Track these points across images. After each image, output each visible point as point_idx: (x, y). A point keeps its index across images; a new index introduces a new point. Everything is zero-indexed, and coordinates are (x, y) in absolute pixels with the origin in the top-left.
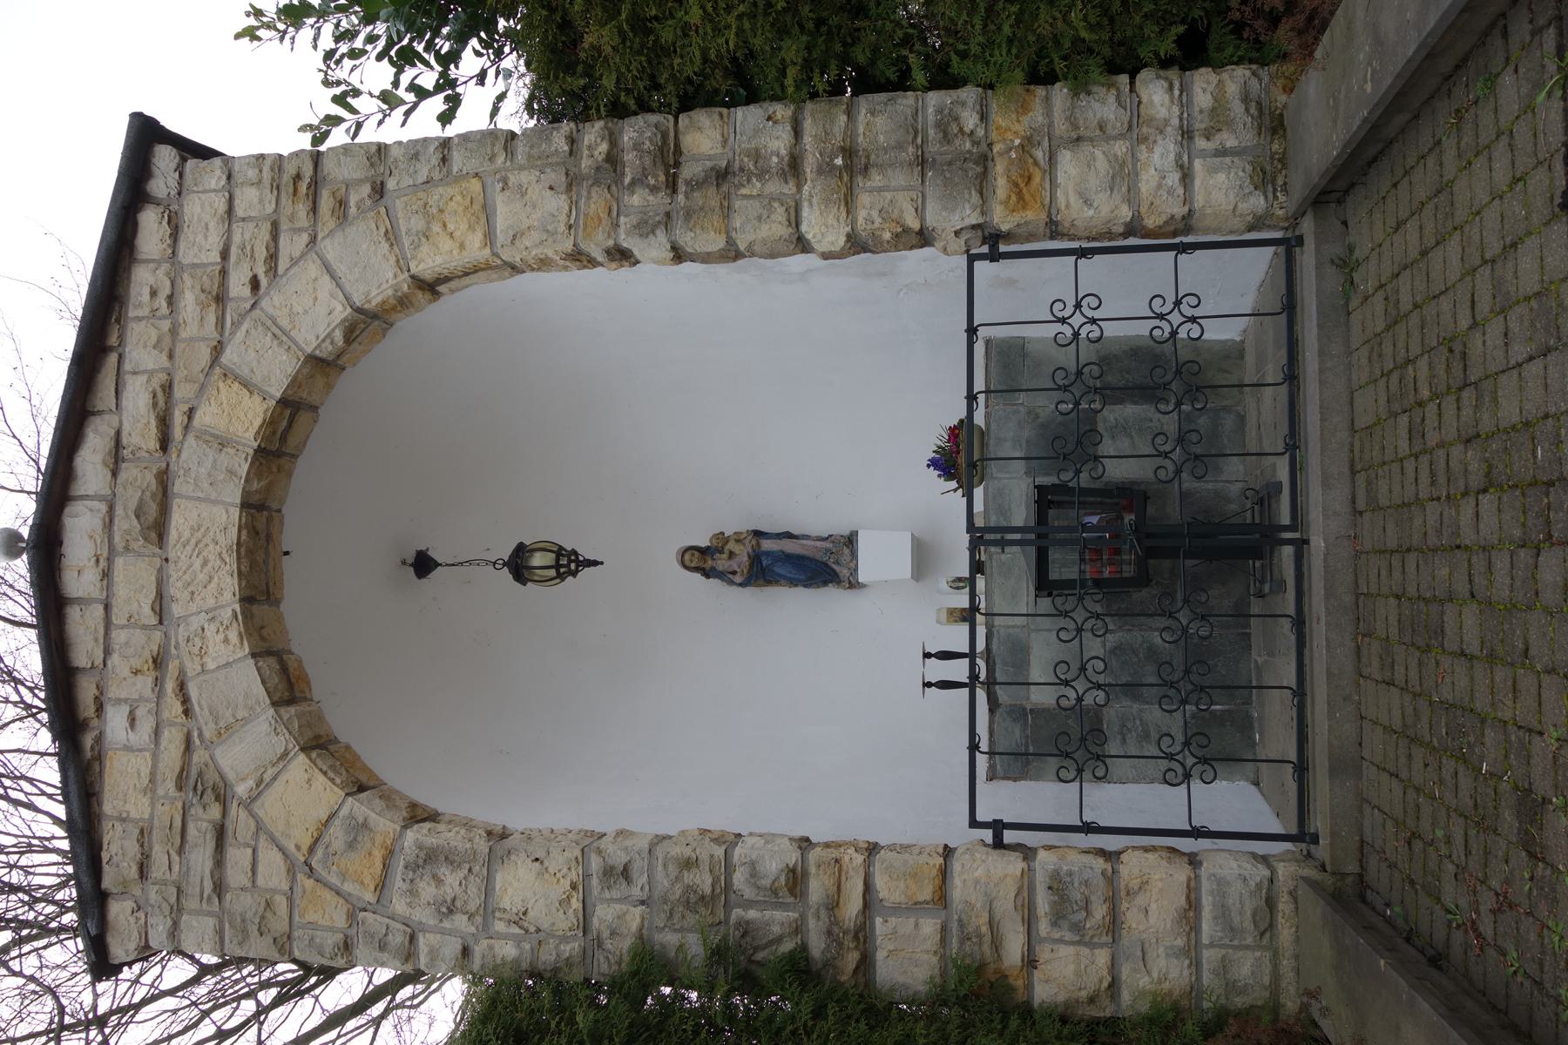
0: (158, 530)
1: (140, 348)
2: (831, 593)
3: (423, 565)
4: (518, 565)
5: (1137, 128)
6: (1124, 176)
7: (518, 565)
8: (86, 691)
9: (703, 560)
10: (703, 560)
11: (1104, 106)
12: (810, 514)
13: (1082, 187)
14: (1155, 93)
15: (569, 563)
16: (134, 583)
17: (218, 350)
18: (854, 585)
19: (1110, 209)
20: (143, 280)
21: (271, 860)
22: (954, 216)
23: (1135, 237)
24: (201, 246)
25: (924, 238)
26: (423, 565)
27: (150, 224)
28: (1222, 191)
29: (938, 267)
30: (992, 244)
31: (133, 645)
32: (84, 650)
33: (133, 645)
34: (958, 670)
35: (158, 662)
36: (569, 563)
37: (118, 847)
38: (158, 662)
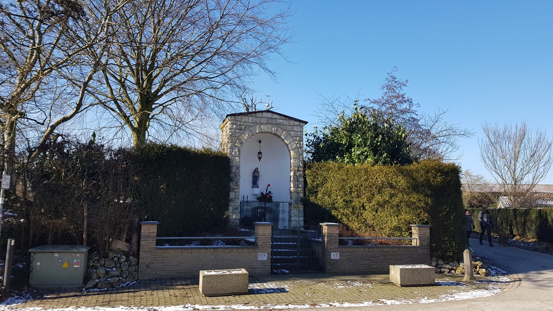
0: (269, 124)
1: (286, 122)
2: (251, 184)
3: (260, 142)
4: (260, 153)
5: (299, 217)
6: (295, 216)
7: (260, 153)
8: (254, 115)
9: (256, 171)
10: (256, 171)
11: (302, 214)
12: (260, 182)
13: (294, 211)
14: (302, 219)
15: (260, 158)
16: (264, 120)
17: (285, 130)
18: (253, 187)
19: (292, 215)
20: (292, 122)
21: (239, 134)
22: (292, 201)
23: (290, 216)
24: (295, 129)
25: (291, 198)
26: (260, 142)
27: (298, 123)
28: (294, 224)
29: (288, 199)
30: (290, 204)
31: (258, 120)
32: (258, 115)
33: (258, 120)
34: (246, 199)
35: (256, 123)
36: (260, 158)
37: (239, 118)
38: (256, 123)
